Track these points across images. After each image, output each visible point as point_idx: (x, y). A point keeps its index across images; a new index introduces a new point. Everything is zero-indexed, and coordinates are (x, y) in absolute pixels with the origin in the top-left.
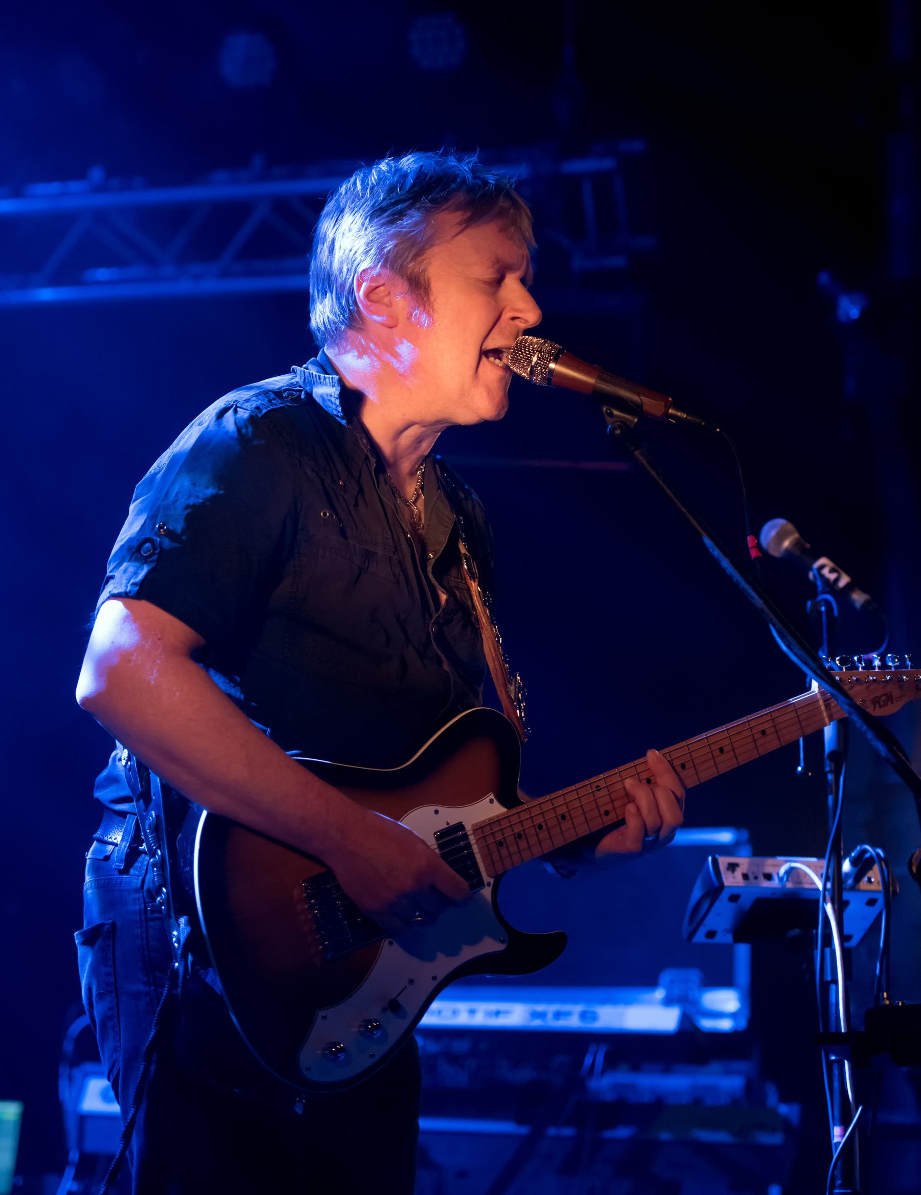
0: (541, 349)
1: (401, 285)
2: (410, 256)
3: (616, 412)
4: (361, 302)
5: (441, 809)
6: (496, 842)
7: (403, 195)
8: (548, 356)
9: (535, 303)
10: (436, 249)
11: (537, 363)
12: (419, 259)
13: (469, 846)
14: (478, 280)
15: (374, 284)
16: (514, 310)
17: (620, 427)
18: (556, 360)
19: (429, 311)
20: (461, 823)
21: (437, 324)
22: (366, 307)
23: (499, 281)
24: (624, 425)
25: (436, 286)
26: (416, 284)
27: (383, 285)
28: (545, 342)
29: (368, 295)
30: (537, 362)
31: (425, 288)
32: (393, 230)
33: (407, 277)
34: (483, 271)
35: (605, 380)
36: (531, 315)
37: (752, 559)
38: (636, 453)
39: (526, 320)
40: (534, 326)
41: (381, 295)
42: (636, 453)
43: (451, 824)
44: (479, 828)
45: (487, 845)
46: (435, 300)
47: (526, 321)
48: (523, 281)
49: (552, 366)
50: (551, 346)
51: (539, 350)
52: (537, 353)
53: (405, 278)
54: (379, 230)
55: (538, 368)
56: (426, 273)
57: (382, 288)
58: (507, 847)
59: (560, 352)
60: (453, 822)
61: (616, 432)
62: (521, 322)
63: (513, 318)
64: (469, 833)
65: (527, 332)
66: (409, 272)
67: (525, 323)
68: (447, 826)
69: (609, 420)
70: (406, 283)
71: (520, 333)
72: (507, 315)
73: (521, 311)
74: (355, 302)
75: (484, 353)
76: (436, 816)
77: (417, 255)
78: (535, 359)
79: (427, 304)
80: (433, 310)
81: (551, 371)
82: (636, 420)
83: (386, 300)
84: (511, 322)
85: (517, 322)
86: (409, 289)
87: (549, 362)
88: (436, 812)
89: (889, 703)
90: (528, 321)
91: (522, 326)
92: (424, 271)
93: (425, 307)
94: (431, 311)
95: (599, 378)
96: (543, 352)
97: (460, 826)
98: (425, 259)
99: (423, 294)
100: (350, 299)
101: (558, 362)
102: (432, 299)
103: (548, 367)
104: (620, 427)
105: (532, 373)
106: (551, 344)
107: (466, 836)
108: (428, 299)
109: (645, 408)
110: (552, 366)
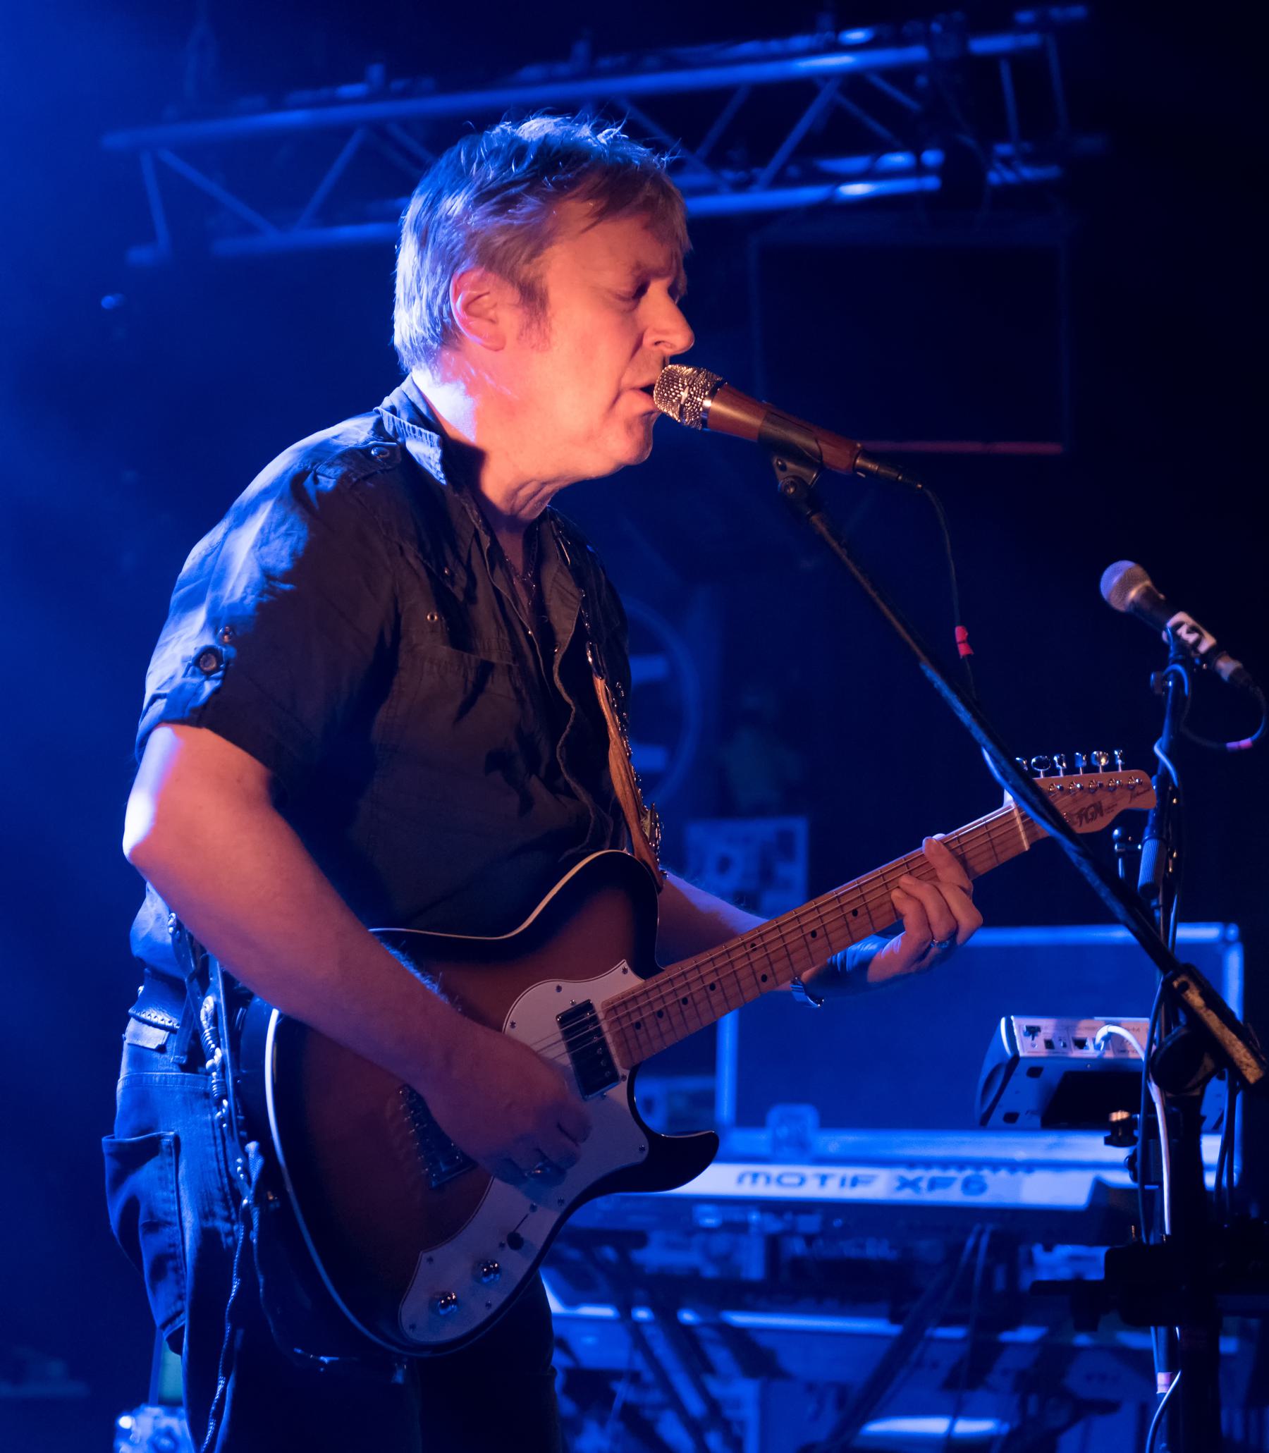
0: (693, 382)
1: (511, 295)
2: (523, 257)
3: (790, 465)
4: (458, 315)
5: (564, 984)
6: (632, 1024)
7: (519, 174)
8: (702, 392)
9: (685, 321)
10: (556, 249)
11: (687, 401)
12: (535, 260)
13: (599, 1031)
14: (609, 291)
15: (475, 293)
17: (792, 484)
18: (712, 396)
19: (544, 330)
20: (589, 1000)
21: (555, 348)
22: (464, 322)
23: (640, 291)
24: (798, 481)
25: (556, 295)
26: (529, 294)
27: (488, 293)
28: (699, 372)
29: (466, 307)
30: (687, 399)
31: (541, 299)
32: (502, 221)
33: (519, 283)
34: (616, 278)
35: (773, 423)
36: (680, 338)
37: (961, 657)
38: (814, 518)
39: (671, 344)
40: (684, 351)
41: (486, 306)
42: (814, 518)
43: (577, 1004)
44: (612, 1008)
45: (622, 1029)
46: (553, 315)
47: (672, 346)
48: (672, 291)
49: (708, 403)
50: (706, 377)
51: (690, 383)
52: (688, 388)
53: (516, 284)
54: (484, 221)
55: (688, 407)
56: (544, 279)
57: (486, 298)
58: (647, 1030)
59: (719, 385)
60: (579, 1001)
61: (788, 491)
62: (666, 346)
63: (657, 343)
64: (601, 1016)
65: (675, 359)
66: (522, 276)
67: (671, 348)
68: (572, 1006)
69: (781, 475)
70: (516, 291)
71: (668, 361)
72: (648, 340)
73: (666, 332)
74: (450, 314)
76: (555, 991)
77: (533, 255)
78: (684, 395)
79: (542, 321)
80: (551, 330)
81: (706, 410)
82: (815, 475)
83: (491, 313)
84: (655, 348)
85: (661, 347)
86: (520, 299)
87: (703, 399)
88: (559, 989)
89: (1098, 815)
90: (675, 346)
91: (669, 352)
92: (541, 276)
93: (539, 324)
94: (547, 330)
95: (767, 419)
96: (696, 386)
97: (588, 1006)
98: (541, 262)
99: (538, 307)
101: (716, 397)
102: (549, 314)
103: (701, 406)
104: (792, 484)
105: (681, 414)
106: (707, 375)
107: (595, 1019)
108: (545, 315)
109: (826, 458)
110: (708, 403)
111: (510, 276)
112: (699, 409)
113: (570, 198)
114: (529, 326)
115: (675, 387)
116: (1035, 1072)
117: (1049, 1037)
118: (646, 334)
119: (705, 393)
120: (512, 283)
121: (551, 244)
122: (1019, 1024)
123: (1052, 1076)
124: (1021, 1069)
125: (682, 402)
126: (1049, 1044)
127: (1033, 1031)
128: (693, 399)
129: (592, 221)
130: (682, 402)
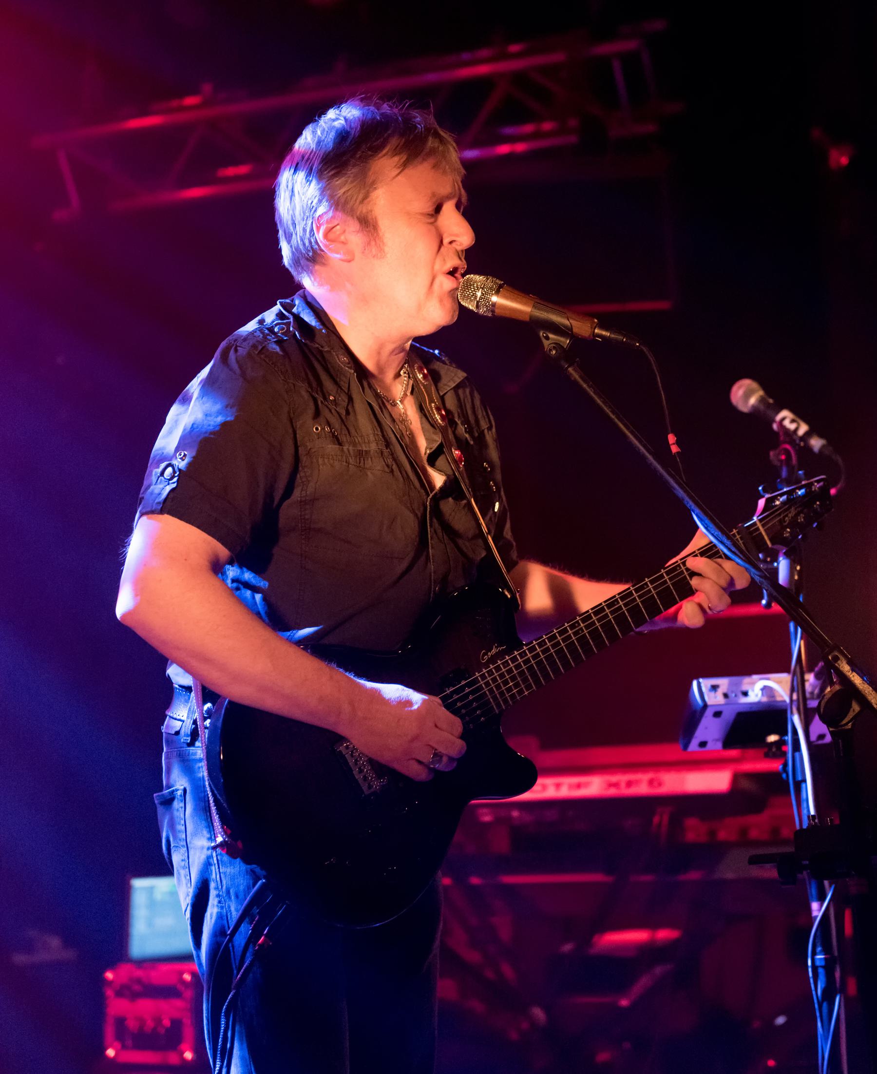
0: (484, 286)
1: (353, 225)
3: (551, 336)
4: (321, 242)
12: (366, 201)
15: (330, 226)
18: (497, 292)
22: (326, 246)
24: (558, 346)
27: (338, 225)
28: (488, 279)
29: (326, 236)
33: (357, 217)
38: (570, 369)
42: (570, 369)
49: (495, 299)
51: (482, 287)
52: (481, 289)
53: (355, 217)
56: (373, 212)
59: (501, 286)
61: (552, 353)
69: (546, 343)
74: (316, 242)
78: (479, 294)
81: (494, 305)
82: (568, 341)
83: (342, 238)
86: (360, 227)
95: (534, 307)
96: (486, 288)
98: (370, 201)
100: (312, 240)
104: (554, 348)
105: (477, 307)
106: (493, 281)
110: (495, 299)
112: (489, 303)
115: (472, 289)
116: (717, 714)
117: (725, 691)
119: (492, 292)
121: (375, 189)
123: (729, 715)
124: (709, 713)
125: (478, 299)
126: (726, 696)
127: (714, 688)
128: (485, 296)
130: (478, 299)
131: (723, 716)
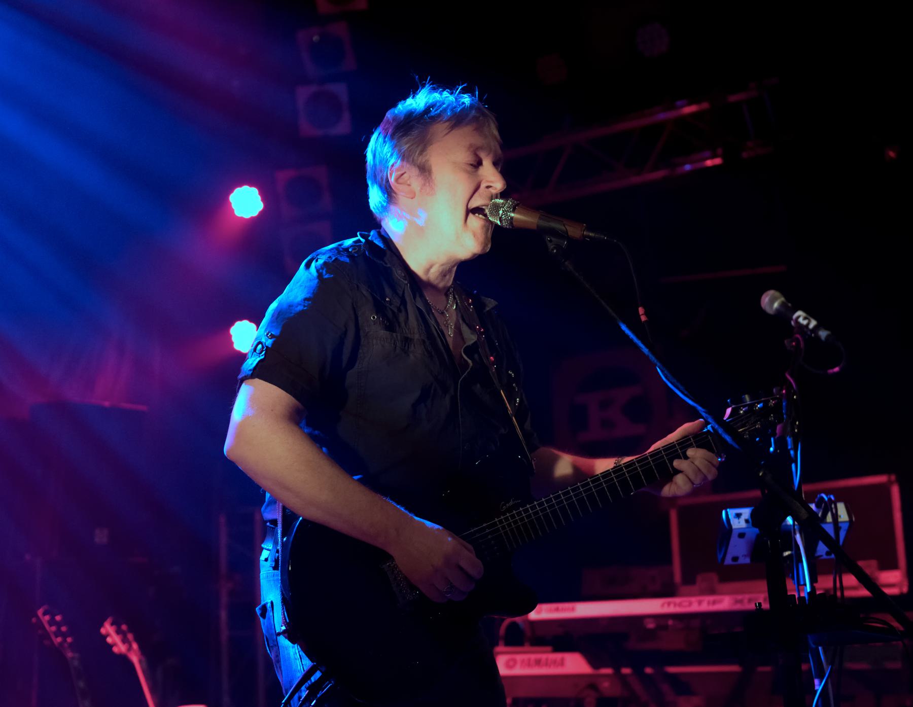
3: (553, 239)
11: (502, 215)
16: (488, 181)
18: (514, 211)
34: (463, 156)
36: (498, 185)
47: (496, 189)
49: (512, 215)
57: (405, 175)
59: (517, 205)
62: (493, 189)
70: (417, 169)
73: (491, 182)
75: (472, 211)
81: (512, 218)
85: (490, 189)
91: (493, 191)
92: (428, 161)
110: (512, 215)
111: (413, 163)
113: (438, 123)
114: (424, 185)
116: (742, 535)
118: (482, 182)
120: (414, 165)
122: (732, 512)
125: (500, 215)
127: (738, 516)
129: (448, 131)
130: (500, 215)
131: (746, 536)
